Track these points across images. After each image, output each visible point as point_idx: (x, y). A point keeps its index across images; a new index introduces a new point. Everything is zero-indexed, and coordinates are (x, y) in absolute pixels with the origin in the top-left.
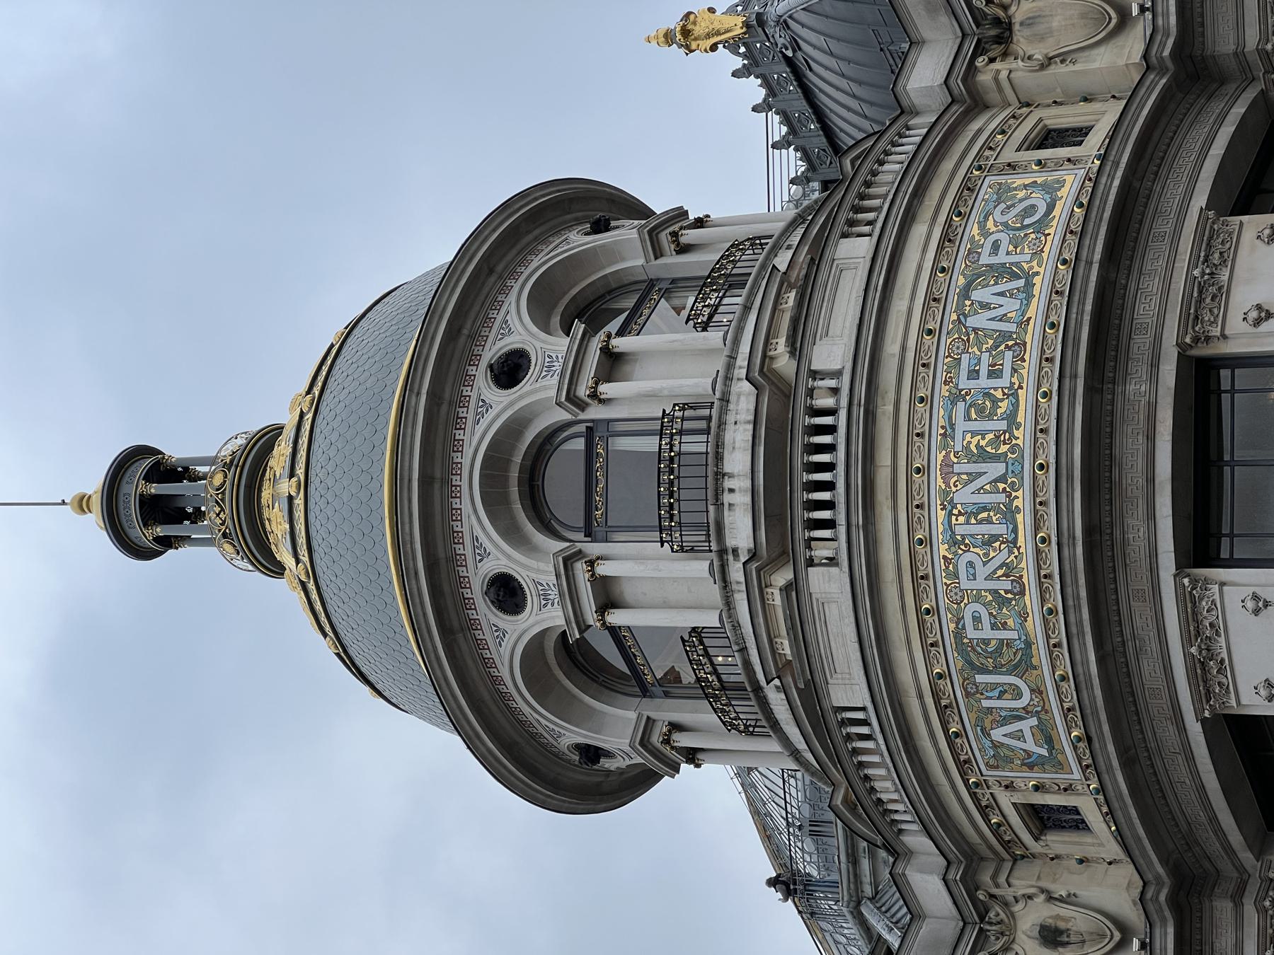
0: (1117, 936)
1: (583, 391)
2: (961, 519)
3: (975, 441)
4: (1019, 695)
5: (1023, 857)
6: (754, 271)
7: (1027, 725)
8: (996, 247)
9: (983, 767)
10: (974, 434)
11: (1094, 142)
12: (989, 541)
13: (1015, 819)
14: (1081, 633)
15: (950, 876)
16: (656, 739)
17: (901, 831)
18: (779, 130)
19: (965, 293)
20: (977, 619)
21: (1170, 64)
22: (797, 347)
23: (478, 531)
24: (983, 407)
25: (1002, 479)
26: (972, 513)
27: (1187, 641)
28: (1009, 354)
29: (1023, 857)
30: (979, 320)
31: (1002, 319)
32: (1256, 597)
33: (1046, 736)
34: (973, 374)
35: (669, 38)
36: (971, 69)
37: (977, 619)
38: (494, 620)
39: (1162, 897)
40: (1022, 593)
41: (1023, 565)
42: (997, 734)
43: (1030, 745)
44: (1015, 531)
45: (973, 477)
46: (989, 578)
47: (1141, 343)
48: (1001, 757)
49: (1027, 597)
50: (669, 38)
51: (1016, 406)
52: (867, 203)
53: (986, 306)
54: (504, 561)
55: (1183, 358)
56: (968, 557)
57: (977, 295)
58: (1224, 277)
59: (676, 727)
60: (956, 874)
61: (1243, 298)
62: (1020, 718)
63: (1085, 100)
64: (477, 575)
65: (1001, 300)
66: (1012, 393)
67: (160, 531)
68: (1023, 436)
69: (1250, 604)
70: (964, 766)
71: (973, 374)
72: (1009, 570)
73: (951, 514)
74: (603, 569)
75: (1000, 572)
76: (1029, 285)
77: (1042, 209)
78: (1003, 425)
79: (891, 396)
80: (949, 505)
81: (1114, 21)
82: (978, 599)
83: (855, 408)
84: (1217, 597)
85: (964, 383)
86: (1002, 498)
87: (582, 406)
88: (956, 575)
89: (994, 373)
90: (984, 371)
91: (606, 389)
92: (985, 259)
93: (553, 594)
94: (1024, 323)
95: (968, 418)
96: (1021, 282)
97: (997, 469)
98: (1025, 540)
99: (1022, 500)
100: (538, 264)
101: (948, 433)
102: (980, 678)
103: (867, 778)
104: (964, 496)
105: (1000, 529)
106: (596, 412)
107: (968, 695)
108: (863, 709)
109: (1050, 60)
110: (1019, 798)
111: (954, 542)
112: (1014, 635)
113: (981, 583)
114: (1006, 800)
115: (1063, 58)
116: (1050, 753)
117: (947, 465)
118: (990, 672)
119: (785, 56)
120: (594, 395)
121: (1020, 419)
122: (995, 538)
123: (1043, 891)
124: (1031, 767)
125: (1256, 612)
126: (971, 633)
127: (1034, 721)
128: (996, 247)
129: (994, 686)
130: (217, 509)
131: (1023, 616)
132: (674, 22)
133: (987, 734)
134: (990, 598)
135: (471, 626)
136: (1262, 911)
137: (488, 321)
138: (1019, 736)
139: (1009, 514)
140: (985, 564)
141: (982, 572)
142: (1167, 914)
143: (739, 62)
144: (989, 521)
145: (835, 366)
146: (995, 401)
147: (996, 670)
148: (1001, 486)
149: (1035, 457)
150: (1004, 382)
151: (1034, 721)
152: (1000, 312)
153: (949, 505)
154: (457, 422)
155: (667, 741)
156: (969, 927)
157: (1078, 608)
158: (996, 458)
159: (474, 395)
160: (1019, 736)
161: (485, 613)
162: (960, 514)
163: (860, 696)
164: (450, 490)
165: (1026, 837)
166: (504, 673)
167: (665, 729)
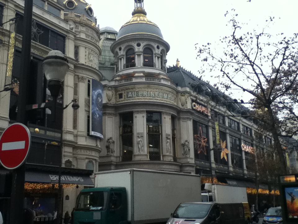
1: (156, 55)
12: (148, 94)
13: (120, 92)
16: (122, 56)
20: (141, 93)
23: (144, 43)
26: (150, 94)
27: (141, 111)
30: (165, 95)
33: (130, 97)
35: (178, 59)
37: (141, 93)
42: (130, 93)
46: (145, 94)
48: (128, 93)
50: (178, 59)
59: (124, 58)
61: (166, 116)
66: (159, 97)
68: (156, 98)
72: (145, 96)
74: (141, 55)
76: (166, 99)
80: (151, 91)
85: (160, 93)
87: (155, 54)
89: (161, 96)
91: (156, 57)
93: (139, 50)
94: (164, 98)
97: (154, 96)
99: (151, 98)
104: (151, 93)
106: (154, 56)
109: (180, 99)
110: (123, 93)
111: (148, 91)
112: (140, 95)
114: (123, 92)
115: (180, 100)
117: (153, 91)
126: (140, 92)
131: (141, 97)
132: (179, 60)
135: (135, 41)
139: (150, 96)
141: (145, 94)
146: (159, 96)
153: (151, 91)
155: (123, 57)
160: (130, 95)
161: (137, 42)
165: (119, 93)
166: (130, 43)
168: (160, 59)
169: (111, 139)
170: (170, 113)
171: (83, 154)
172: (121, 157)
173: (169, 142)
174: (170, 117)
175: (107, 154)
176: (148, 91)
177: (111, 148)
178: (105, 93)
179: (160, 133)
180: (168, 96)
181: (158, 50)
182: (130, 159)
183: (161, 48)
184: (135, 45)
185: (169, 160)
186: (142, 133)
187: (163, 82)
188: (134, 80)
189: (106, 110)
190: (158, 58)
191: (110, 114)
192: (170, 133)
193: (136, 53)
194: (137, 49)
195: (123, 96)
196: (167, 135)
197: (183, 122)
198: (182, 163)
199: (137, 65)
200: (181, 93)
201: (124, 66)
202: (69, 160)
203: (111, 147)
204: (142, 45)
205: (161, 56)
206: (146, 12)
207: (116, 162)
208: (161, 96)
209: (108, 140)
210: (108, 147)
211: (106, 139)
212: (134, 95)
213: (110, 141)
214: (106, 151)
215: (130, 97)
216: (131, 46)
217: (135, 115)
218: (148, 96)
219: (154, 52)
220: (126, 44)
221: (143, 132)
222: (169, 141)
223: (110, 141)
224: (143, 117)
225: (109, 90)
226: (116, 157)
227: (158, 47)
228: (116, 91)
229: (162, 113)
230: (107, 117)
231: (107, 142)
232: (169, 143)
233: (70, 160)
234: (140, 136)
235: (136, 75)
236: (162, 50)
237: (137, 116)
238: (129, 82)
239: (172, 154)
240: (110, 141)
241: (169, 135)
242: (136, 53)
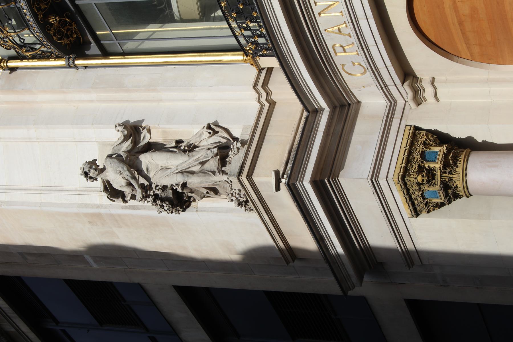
177: (180, 179)
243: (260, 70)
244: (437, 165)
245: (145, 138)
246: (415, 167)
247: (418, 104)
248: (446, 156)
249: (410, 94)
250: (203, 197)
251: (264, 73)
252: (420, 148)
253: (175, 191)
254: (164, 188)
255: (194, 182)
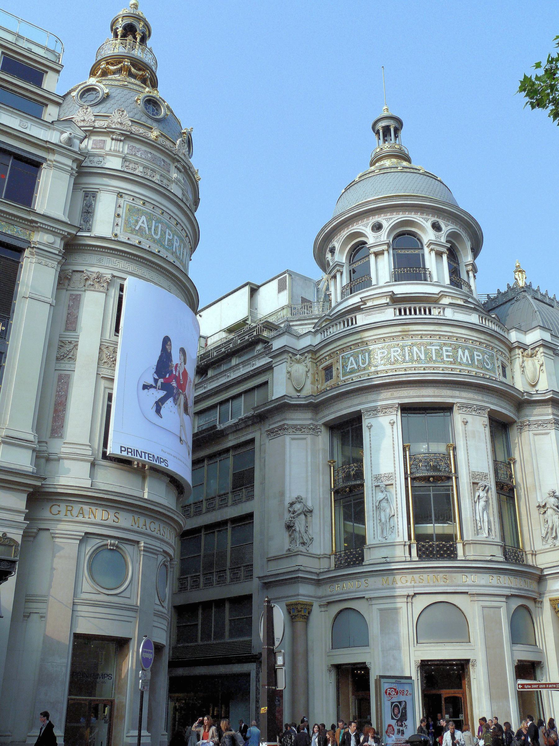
0: (299, 389)
2: (409, 348)
3: (430, 351)
4: (363, 364)
5: (317, 365)
6: (463, 291)
7: (355, 366)
8: (479, 356)
9: (342, 355)
10: (431, 351)
11: (504, 380)
12: (404, 355)
13: (327, 363)
14: (383, 380)
15: (311, 347)
17: (321, 333)
18: (492, 296)
19: (468, 349)
21: (524, 398)
22: (451, 304)
24: (439, 353)
25: (421, 359)
26: (411, 351)
28: (452, 360)
29: (317, 365)
31: (461, 358)
32: (394, 423)
33: (352, 371)
34: (447, 351)
36: (519, 348)
38: (370, 224)
39: (312, 400)
40: (391, 364)
41: (398, 365)
42: (352, 358)
43: (349, 367)
44: (407, 362)
45: (421, 351)
46: (394, 356)
47: (457, 393)
49: (390, 366)
51: (439, 362)
52: (487, 321)
53: (464, 354)
54: (386, 227)
55: (453, 404)
56: (399, 351)
57: (466, 351)
58: (474, 413)
60: (311, 348)
61: (469, 418)
62: (357, 364)
63: (513, 377)
64: (380, 219)
65: (466, 357)
66: (443, 361)
67: (381, 131)
69: (392, 422)
70: (342, 350)
71: (447, 351)
72: (397, 361)
73: (410, 346)
74: (386, 253)
75: (396, 359)
77: (488, 367)
78: (434, 358)
79: (440, 329)
80: (413, 345)
81: (533, 384)
82: (388, 353)
83: (437, 320)
84: (393, 413)
85: (444, 348)
86: (415, 358)
87: (428, 247)
88: (394, 347)
89: (448, 356)
90: (447, 353)
91: (433, 253)
92: (475, 353)
93: (378, 240)
94: (460, 364)
95: (436, 350)
96: (470, 362)
97: (423, 357)
98: (405, 365)
99: (415, 365)
100: (464, 235)
101: (431, 344)
102: (367, 354)
103: (336, 325)
104: (415, 349)
105: (407, 358)
106: (426, 250)
107: (362, 351)
108: (356, 323)
113: (393, 354)
116: (348, 372)
118: (369, 356)
119: (514, 298)
120: (432, 250)
121: (436, 363)
122: (405, 357)
123: (309, 370)
124: (343, 367)
125: (390, 423)
127: (356, 368)
128: (479, 356)
129: (365, 358)
130: (389, 147)
131: (385, 365)
133: (352, 356)
134: (389, 356)
136: (309, 425)
137: (448, 220)
138: (352, 364)
139: (412, 360)
140: (398, 355)
141: (395, 354)
142: (307, 402)
143: (511, 285)
144: (409, 355)
145: (446, 315)
147: (370, 358)
148: (419, 359)
149: (427, 367)
150: (445, 359)
151: (356, 368)
152: (463, 358)
153: (413, 345)
154: (422, 213)
155: (338, 271)
156: (297, 352)
157: (389, 379)
158: (426, 357)
159: (430, 217)
162: (411, 348)
163: (359, 323)
164: (404, 211)
167: (341, 270)
168: (445, 257)
169: (300, 502)
170: (482, 408)
171: (139, 530)
172: (333, 557)
173: (484, 499)
174: (486, 420)
175: (289, 550)
176: (403, 348)
177: (298, 529)
178: (285, 371)
179: (451, 472)
180: (472, 359)
181: (437, 233)
182: (359, 560)
183: (447, 228)
184: (368, 231)
185: (489, 558)
186: (389, 477)
187: (449, 314)
188: (362, 319)
189: (285, 419)
190: (439, 254)
191: (297, 429)
192: (486, 471)
193: (372, 250)
194: (371, 238)
195: (334, 373)
196: (474, 475)
197: (536, 437)
198: (542, 567)
199: (374, 282)
200: (525, 350)
201: (342, 293)
202: (4, 534)
203: (300, 524)
204: (386, 225)
205: (449, 249)
206: (405, 154)
207: (318, 574)
208: (448, 356)
209: (292, 504)
210: (289, 527)
211: (288, 501)
212: (363, 364)
213: (297, 507)
214: (287, 540)
215: (352, 371)
216: (359, 234)
217: (365, 422)
218: (404, 361)
219: (425, 240)
220: (345, 233)
221: (393, 471)
222: (482, 494)
223: (296, 509)
224: (392, 424)
225: (298, 362)
226: (319, 558)
227: (436, 227)
228: (316, 361)
229: (455, 408)
230: (288, 438)
231: (290, 511)
232: (482, 503)
233: (9, 535)
234: (382, 485)
235: (369, 304)
236: (453, 236)
237: (373, 423)
238: (349, 328)
239: (498, 539)
240: (297, 507)
241: (486, 476)
242: (372, 250)
243: (330, 555)
244: (303, 613)
245: (309, 515)
246: (302, 607)
247: (319, 606)
248: (305, 616)
249: (322, 604)
250: (290, 536)
251: (329, 556)
252: (307, 607)
253: (293, 526)
254: (294, 523)
255: (297, 535)
